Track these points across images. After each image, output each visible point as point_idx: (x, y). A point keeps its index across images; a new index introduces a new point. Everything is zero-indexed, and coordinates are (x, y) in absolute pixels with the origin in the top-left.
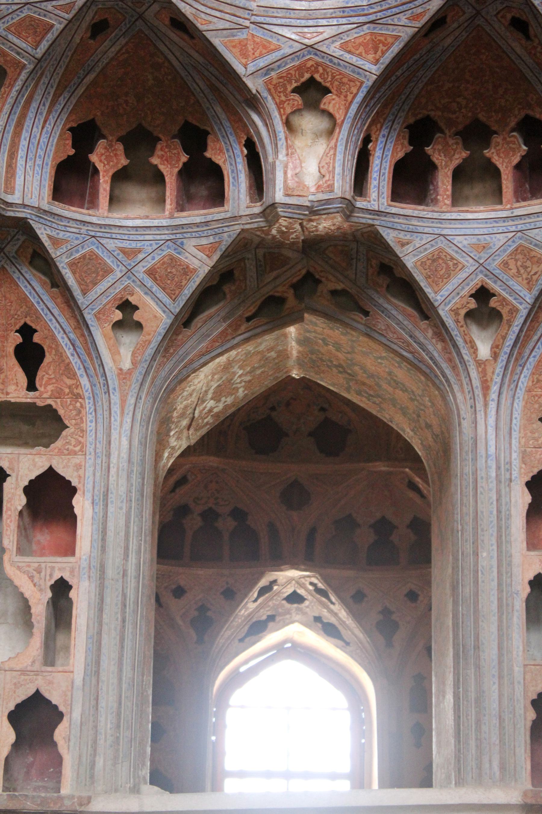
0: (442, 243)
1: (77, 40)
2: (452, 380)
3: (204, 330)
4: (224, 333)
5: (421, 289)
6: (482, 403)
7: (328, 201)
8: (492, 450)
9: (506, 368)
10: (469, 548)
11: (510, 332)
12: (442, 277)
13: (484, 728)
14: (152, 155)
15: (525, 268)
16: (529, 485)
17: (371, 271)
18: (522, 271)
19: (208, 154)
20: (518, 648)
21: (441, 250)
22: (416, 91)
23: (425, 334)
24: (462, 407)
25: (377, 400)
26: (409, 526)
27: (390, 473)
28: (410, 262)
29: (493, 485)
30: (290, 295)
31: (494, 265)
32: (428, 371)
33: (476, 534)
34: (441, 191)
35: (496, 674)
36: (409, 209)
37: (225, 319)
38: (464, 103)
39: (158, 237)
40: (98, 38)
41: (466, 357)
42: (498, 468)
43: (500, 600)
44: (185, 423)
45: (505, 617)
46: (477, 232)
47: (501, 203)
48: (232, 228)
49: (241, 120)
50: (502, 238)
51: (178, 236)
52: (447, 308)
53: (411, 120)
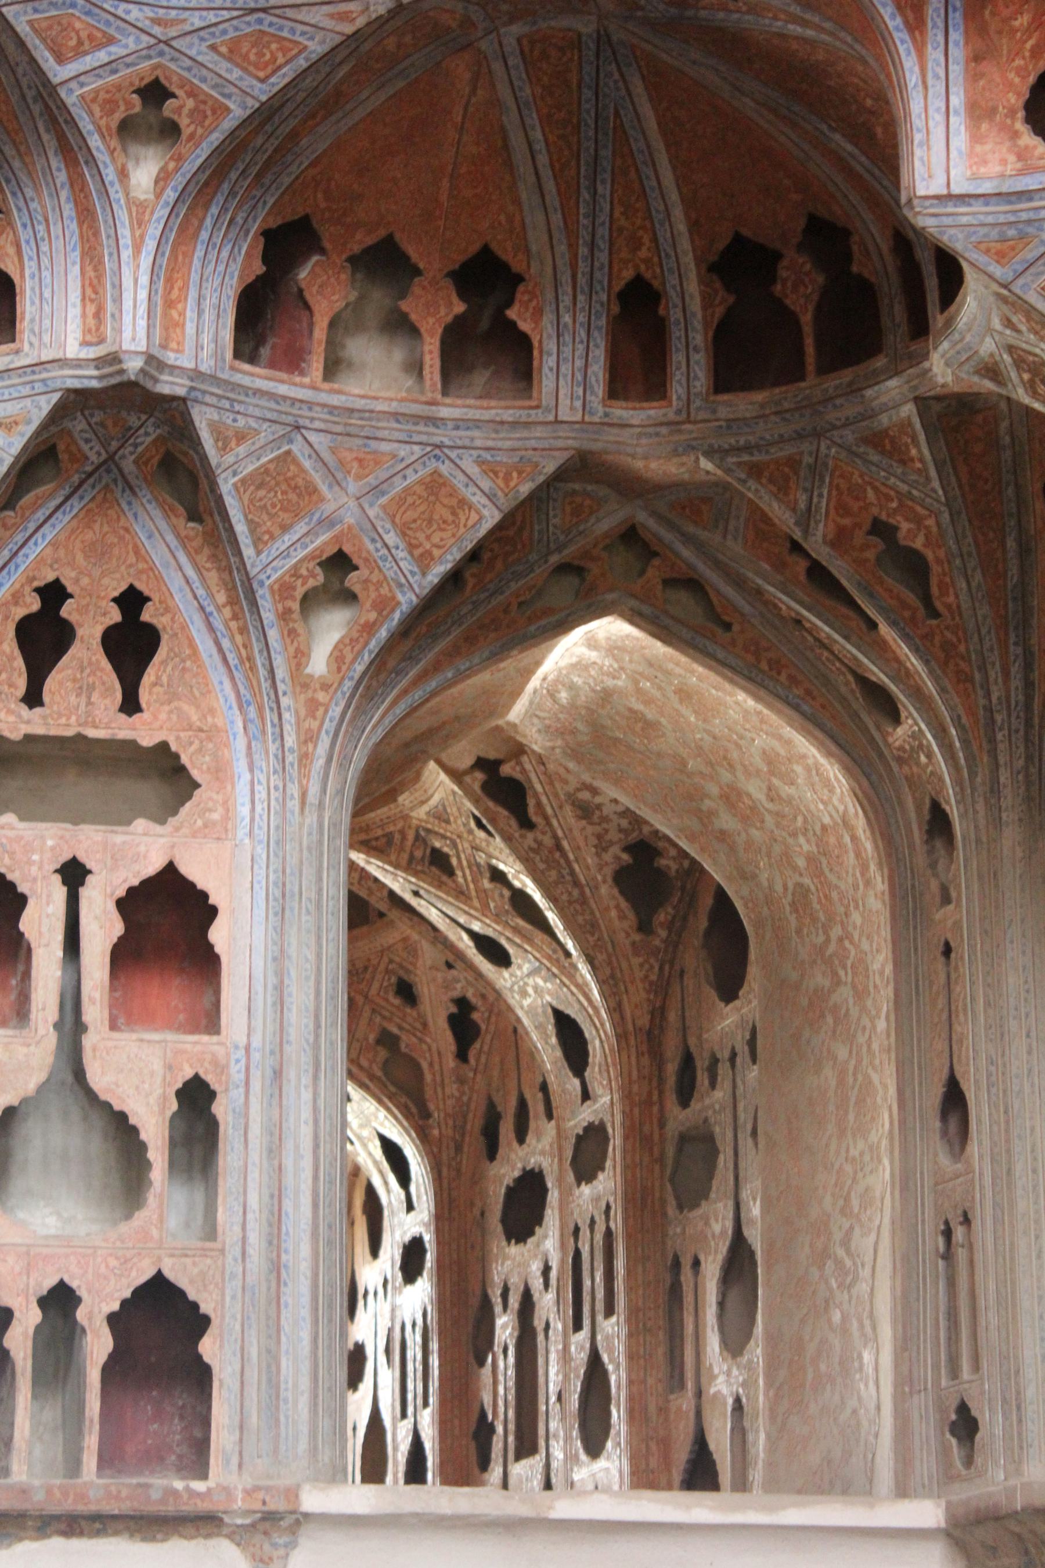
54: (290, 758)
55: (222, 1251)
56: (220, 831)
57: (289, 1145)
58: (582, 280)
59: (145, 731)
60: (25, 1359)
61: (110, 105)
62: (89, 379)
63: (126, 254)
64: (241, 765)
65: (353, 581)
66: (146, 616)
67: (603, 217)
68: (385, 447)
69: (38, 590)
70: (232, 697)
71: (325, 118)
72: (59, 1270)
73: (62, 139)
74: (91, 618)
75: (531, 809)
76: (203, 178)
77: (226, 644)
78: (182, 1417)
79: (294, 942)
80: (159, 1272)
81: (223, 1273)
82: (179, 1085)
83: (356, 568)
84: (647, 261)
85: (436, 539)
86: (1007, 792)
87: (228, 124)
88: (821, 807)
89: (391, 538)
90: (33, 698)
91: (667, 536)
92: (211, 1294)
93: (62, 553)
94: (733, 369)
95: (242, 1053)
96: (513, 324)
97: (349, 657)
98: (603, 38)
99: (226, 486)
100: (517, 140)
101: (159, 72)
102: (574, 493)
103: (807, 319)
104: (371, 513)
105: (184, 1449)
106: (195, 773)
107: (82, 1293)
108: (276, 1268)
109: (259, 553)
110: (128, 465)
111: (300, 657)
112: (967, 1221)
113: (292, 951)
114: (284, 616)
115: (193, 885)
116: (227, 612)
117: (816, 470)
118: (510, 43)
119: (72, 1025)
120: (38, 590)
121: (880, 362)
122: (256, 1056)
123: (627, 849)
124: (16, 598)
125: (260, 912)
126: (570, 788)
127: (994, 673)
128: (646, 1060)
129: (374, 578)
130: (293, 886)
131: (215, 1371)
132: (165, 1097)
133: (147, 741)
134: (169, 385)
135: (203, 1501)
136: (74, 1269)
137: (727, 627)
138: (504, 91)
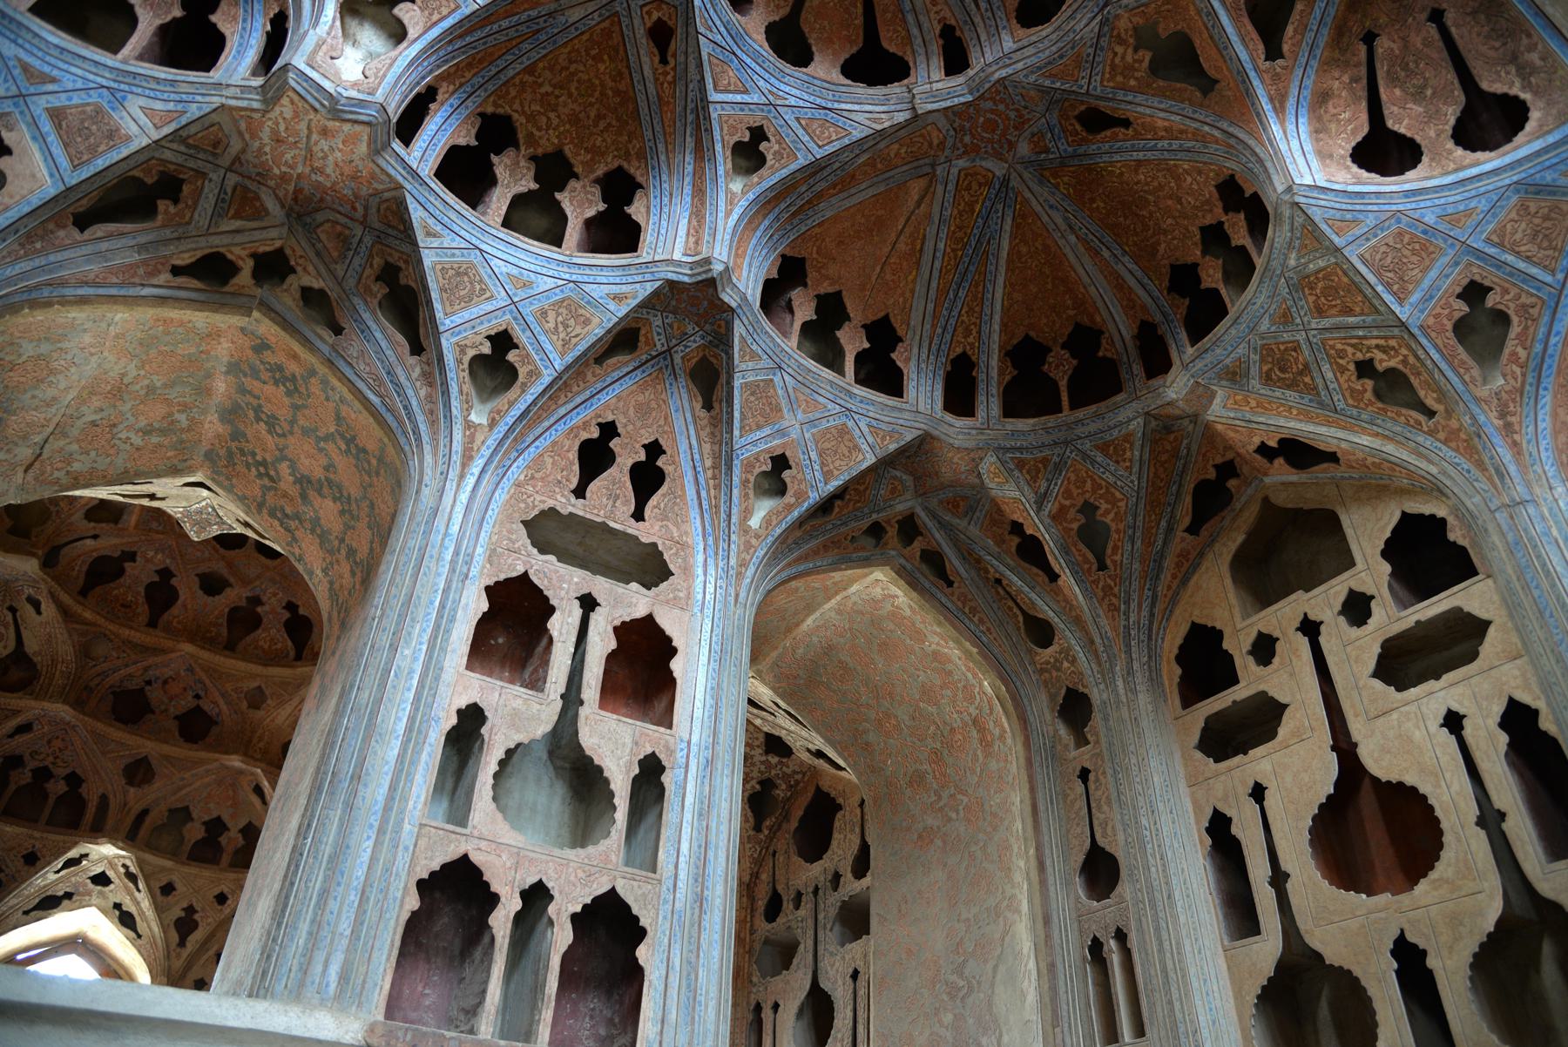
0: (475, 257)
2: (425, 438)
3: (104, 246)
4: (132, 267)
5: (429, 302)
6: (458, 471)
7: (362, 103)
8: (455, 529)
9: (501, 443)
10: (385, 640)
12: (461, 299)
13: (333, 905)
15: (566, 326)
16: (488, 589)
17: (368, 271)
18: (561, 328)
19: (213, 18)
20: (418, 797)
21: (472, 266)
22: (511, 73)
23: (409, 370)
24: (428, 471)
25: (293, 524)
26: (241, 831)
27: (241, 772)
28: (429, 259)
30: (247, 266)
32: (394, 425)
33: (402, 617)
34: (493, 206)
35: (376, 824)
36: (450, 198)
37: (141, 248)
38: (555, 122)
39: (91, 77)
42: (456, 553)
43: (411, 719)
46: (522, 264)
47: (560, 246)
48: (207, 99)
50: (551, 283)
51: (122, 86)
53: (490, 110)
55: (660, 881)
56: (683, 603)
57: (714, 812)
58: (934, 348)
59: (646, 532)
61: (733, 130)
63: (721, 215)
64: (700, 571)
65: (786, 475)
66: (659, 463)
68: (821, 399)
69: (599, 424)
71: (841, 191)
74: (627, 453)
77: (704, 494)
78: (592, 1017)
84: (972, 345)
85: (837, 463)
86: (1139, 675)
87: (794, 167)
89: (814, 455)
90: (580, 492)
91: (930, 524)
94: (1009, 411)
98: (1005, 182)
99: (737, 383)
100: (929, 245)
102: (895, 478)
103: (1063, 384)
104: (807, 435)
106: (671, 567)
107: (555, 893)
108: (700, 900)
110: (678, 359)
111: (747, 513)
112: (1121, 936)
114: (745, 482)
115: (662, 631)
116: (710, 473)
117: (1058, 468)
118: (955, 171)
119: (572, 698)
120: (599, 424)
121: (1119, 398)
122: (694, 749)
123: (760, 783)
124: (585, 425)
125: (704, 659)
127: (1134, 605)
129: (800, 476)
132: (631, 762)
137: (950, 584)
138: (936, 209)
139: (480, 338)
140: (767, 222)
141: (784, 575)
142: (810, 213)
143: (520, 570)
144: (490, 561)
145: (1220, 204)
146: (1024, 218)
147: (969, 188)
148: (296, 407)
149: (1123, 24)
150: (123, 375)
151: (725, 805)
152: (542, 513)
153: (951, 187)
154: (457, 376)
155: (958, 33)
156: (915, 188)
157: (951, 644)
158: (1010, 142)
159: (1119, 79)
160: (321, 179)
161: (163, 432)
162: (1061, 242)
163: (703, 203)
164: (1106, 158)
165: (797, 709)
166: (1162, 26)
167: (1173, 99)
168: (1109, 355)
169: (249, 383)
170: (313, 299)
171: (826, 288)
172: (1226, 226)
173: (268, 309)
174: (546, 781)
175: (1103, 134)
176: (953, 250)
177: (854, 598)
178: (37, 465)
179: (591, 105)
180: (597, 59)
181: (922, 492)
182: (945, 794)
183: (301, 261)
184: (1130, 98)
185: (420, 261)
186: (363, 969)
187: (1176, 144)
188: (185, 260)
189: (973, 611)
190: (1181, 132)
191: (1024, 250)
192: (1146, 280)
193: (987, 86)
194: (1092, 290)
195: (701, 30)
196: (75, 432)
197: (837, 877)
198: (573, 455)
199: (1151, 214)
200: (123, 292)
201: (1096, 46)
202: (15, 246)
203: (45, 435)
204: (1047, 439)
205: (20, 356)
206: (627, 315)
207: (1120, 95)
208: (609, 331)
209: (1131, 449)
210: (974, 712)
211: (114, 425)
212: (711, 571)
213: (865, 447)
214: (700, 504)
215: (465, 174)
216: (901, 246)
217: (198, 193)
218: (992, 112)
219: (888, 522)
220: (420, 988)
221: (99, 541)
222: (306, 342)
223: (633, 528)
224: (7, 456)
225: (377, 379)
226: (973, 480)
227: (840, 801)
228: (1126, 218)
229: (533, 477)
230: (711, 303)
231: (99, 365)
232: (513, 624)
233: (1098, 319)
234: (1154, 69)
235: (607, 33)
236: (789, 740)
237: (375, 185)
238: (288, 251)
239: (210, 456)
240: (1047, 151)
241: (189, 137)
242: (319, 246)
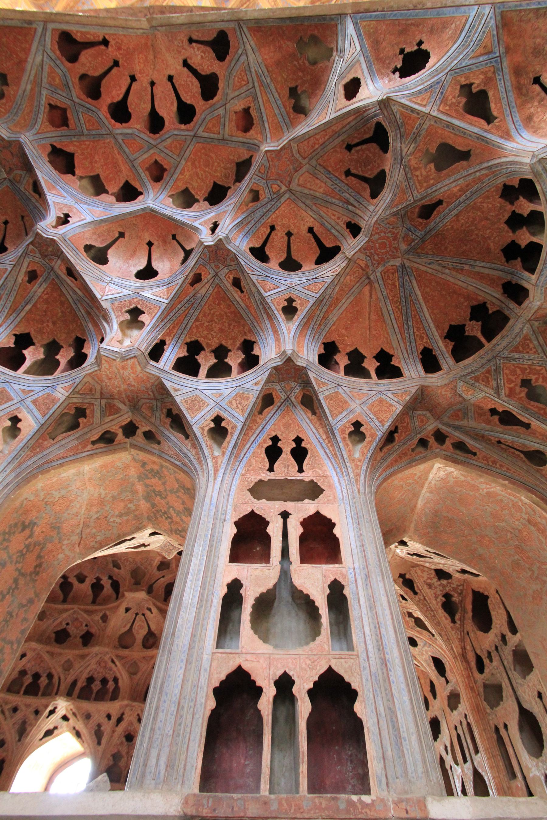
0: (197, 392)
1: (20, 280)
2: (199, 470)
3: (63, 442)
4: (76, 447)
5: (184, 415)
11: (232, 439)
14: (57, 354)
15: (241, 404)
18: (239, 405)
22: (190, 324)
23: (186, 446)
28: (178, 399)
29: (211, 520)
30: (120, 432)
31: (223, 404)
38: (215, 334)
40: (32, 283)
41: (206, 454)
42: (217, 511)
44: (75, 538)
45: (203, 609)
49: (100, 329)
50: (230, 390)
52: (198, 426)
53: (188, 340)
54: (352, 480)
55: (357, 655)
58: (409, 352)
60: (268, 715)
62: (278, 362)
64: (337, 485)
65: (362, 429)
66: (303, 445)
67: (411, 333)
69: (270, 439)
70: (332, 467)
72: (283, 666)
73: (268, 314)
74: (287, 446)
75: (416, 588)
76: (305, 320)
77: (327, 451)
78: (351, 762)
79: (364, 531)
80: (330, 667)
81: (360, 666)
82: (329, 583)
83: (363, 425)
84: (426, 342)
85: (385, 415)
87: (309, 305)
88: (517, 523)
90: (271, 469)
92: (355, 678)
93: (276, 427)
95: (351, 571)
96: (393, 365)
97: (365, 452)
98: (403, 266)
99: (321, 397)
101: (291, 295)
102: (420, 415)
104: (365, 409)
105: (354, 782)
106: (323, 487)
107: (294, 678)
109: (333, 419)
110: (293, 399)
111: (350, 453)
113: (364, 533)
114: (344, 439)
116: (327, 441)
117: (497, 371)
118: (378, 274)
120: (270, 439)
121: (510, 323)
122: (357, 571)
123: (443, 596)
124: (265, 441)
126: (425, 579)
128: (464, 663)
129: (369, 427)
130: (360, 514)
131: (364, 722)
133: (307, 480)
134: (300, 363)
135: (370, 811)
136: (290, 665)
137: (475, 454)
138: (379, 294)
139: (208, 422)
140: (309, 332)
141: (384, 476)
142: (327, 321)
143: (250, 510)
144: (235, 511)
145: (507, 203)
146: (420, 276)
147: (388, 278)
148: (164, 483)
149: (413, 162)
150: (100, 495)
151: (384, 599)
152: (256, 483)
153: (381, 282)
154: (204, 440)
155: (353, 222)
156: (367, 290)
157: (493, 485)
158: (395, 248)
159: (425, 184)
160: (133, 388)
161: (127, 514)
162: (443, 276)
163: (278, 335)
164: (441, 225)
165: (436, 549)
166: (430, 148)
167: (454, 174)
168: (495, 310)
169: (148, 482)
170: (149, 436)
171: (349, 349)
172: (517, 211)
173: (133, 446)
174: (293, 614)
175: (433, 215)
176: (397, 307)
177: (433, 482)
178: (82, 542)
179: (225, 322)
180: (219, 304)
181: (438, 418)
182: (535, 568)
183: (140, 423)
184: (434, 189)
185: (176, 402)
186: (183, 757)
187: (468, 193)
188: (96, 437)
189: (494, 462)
190: (467, 186)
191: (428, 290)
192: (493, 265)
193: (371, 229)
194: (470, 288)
195: (249, 272)
196: (92, 524)
197: (503, 637)
198: (264, 455)
199: (477, 235)
200: (75, 457)
201: (407, 180)
202: (29, 452)
203: (80, 529)
204: (484, 361)
205: (55, 498)
206: (262, 388)
207: (429, 191)
208: (258, 398)
209: (531, 342)
210: (526, 517)
211: (106, 517)
212: (343, 483)
213: (395, 403)
214: (328, 456)
215: (187, 366)
216: (373, 317)
217: (93, 411)
218: (379, 239)
219: (427, 436)
220: (242, 761)
221: (166, 577)
222: (150, 452)
223: (300, 476)
224: (69, 541)
225: (177, 455)
226: (458, 399)
227: (486, 593)
228: (466, 245)
229: (248, 470)
230: (295, 369)
231: (89, 493)
232: (250, 538)
233: (481, 298)
234: (439, 169)
235: (218, 293)
236: (445, 569)
237: (151, 381)
238: (134, 422)
239: (149, 518)
240: (413, 240)
241: (79, 391)
242: (144, 414)
